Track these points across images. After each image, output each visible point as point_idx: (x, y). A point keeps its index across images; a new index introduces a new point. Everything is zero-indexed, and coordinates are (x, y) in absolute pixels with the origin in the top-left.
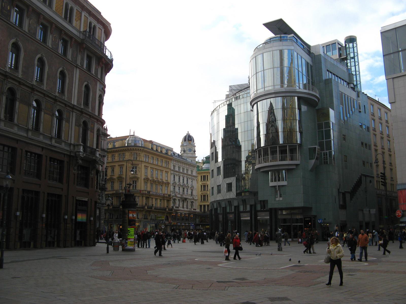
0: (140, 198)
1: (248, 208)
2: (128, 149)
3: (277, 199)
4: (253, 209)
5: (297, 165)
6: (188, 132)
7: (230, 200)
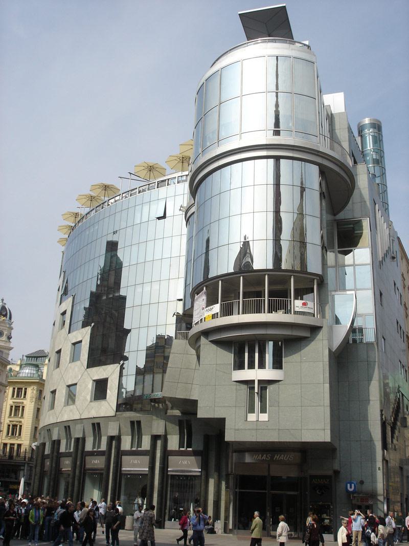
1: (146, 444)
3: (252, 417)
4: (159, 443)
6: (3, 300)
7: (96, 421)
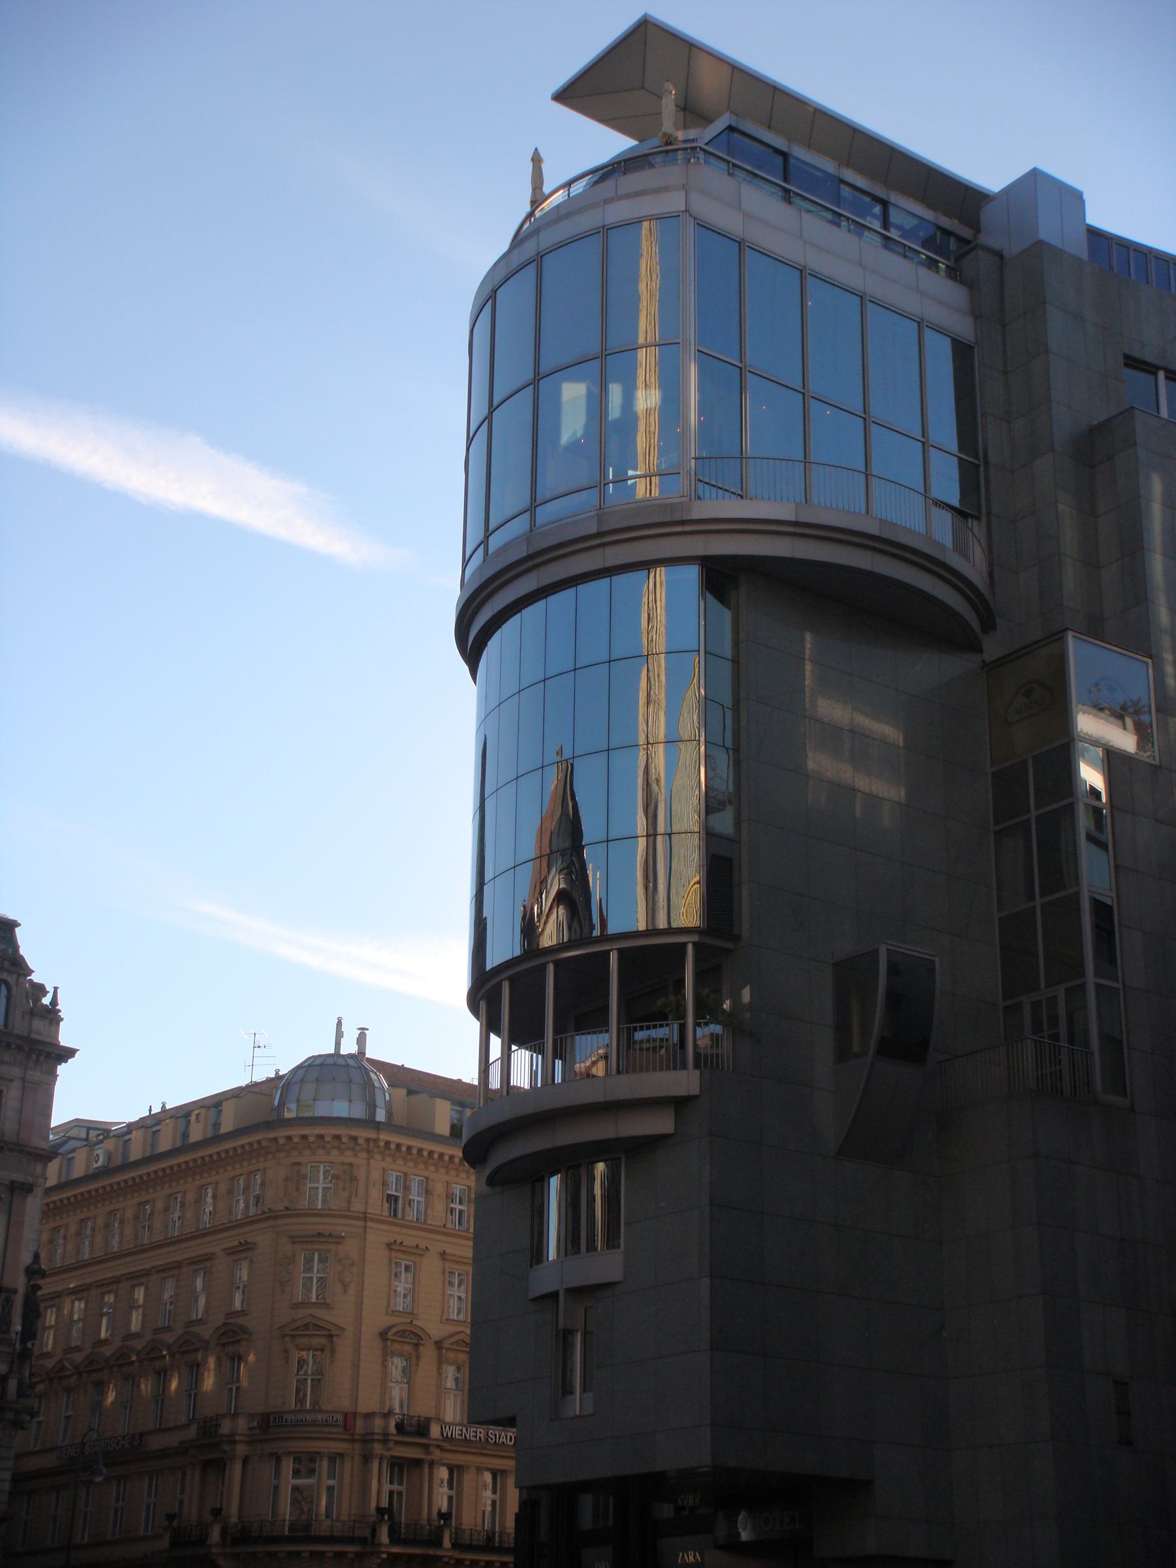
0: (347, 1466)
2: (275, 1140)
5: (680, 1104)
